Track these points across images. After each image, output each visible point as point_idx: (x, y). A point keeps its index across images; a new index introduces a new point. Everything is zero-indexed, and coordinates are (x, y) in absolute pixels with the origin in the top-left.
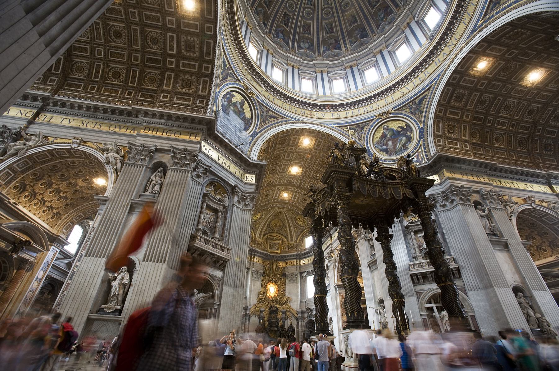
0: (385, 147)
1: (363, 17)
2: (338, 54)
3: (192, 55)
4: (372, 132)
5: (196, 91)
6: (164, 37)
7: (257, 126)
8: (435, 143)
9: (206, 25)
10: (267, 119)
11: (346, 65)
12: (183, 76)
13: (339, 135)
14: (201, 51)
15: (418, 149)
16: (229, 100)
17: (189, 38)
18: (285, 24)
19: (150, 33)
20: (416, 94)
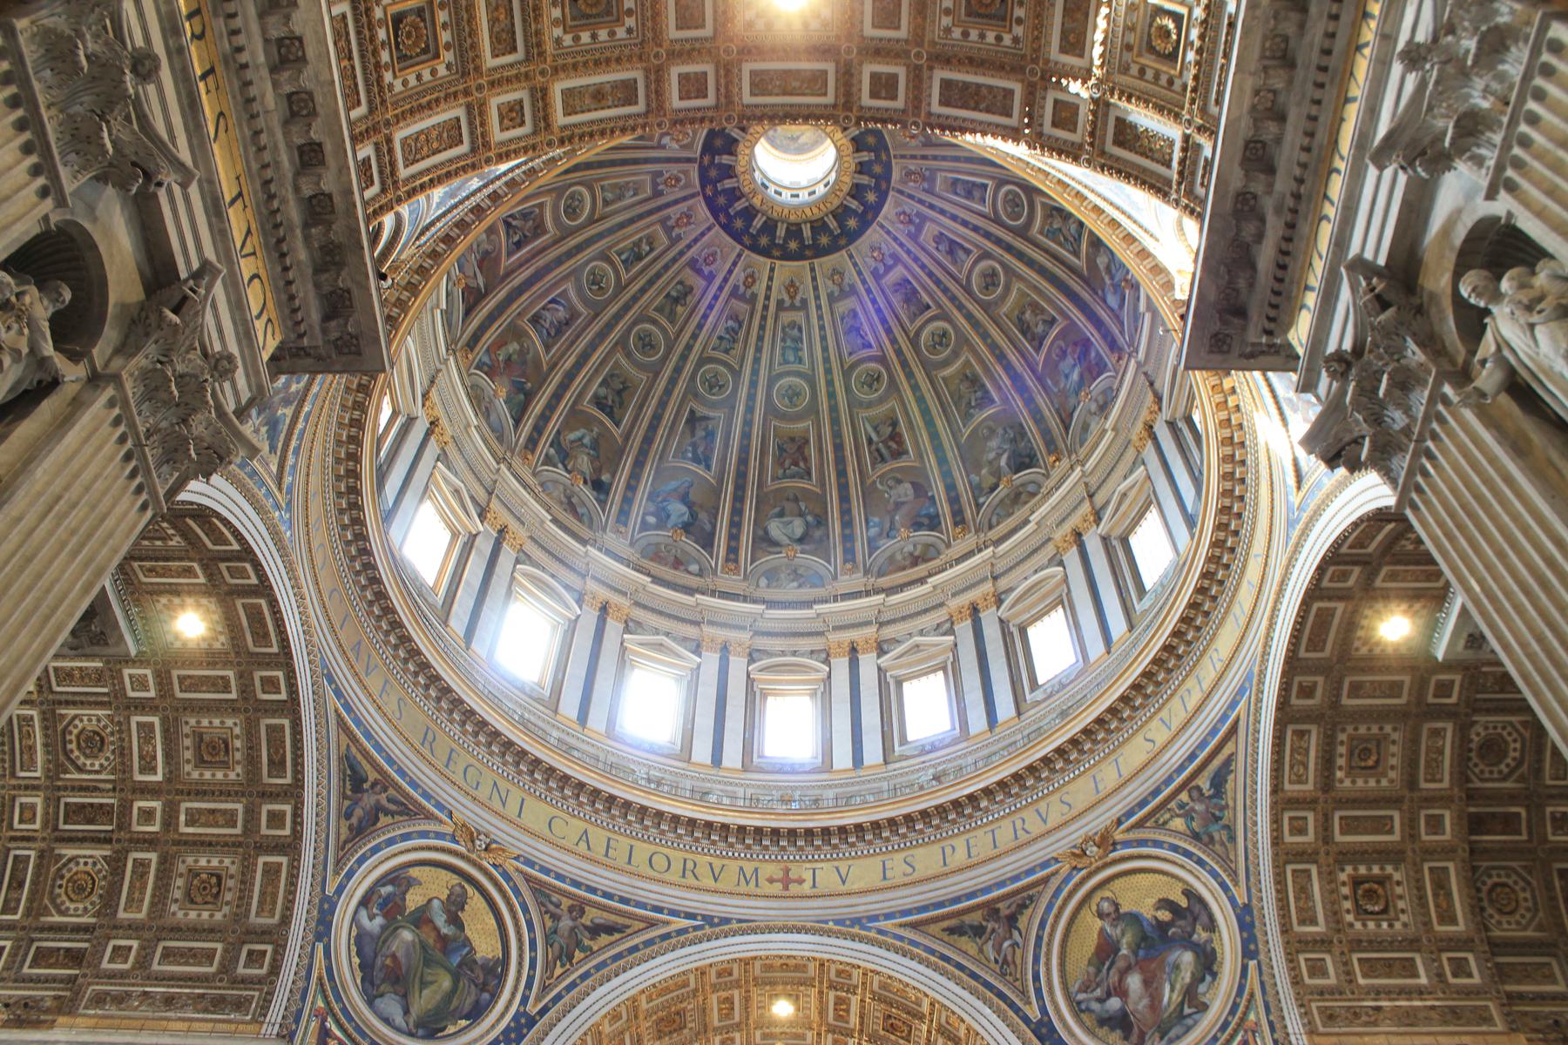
0: (1114, 1003)
1: (1008, 382)
2: (928, 546)
3: (220, 775)
4: (1052, 935)
5: (240, 915)
6: (120, 731)
7: (529, 985)
8: (1296, 981)
9: (258, 675)
10: (578, 944)
11: (954, 604)
12: (190, 860)
13: (914, 964)
14: (252, 761)
15: (1245, 1014)
16: (392, 909)
17: (205, 722)
18: (696, 460)
19: (77, 722)
20: (1192, 757)
